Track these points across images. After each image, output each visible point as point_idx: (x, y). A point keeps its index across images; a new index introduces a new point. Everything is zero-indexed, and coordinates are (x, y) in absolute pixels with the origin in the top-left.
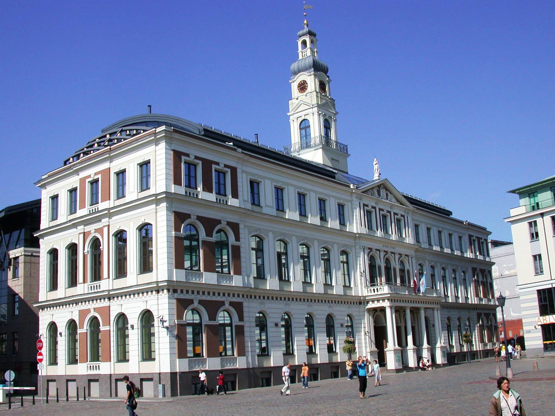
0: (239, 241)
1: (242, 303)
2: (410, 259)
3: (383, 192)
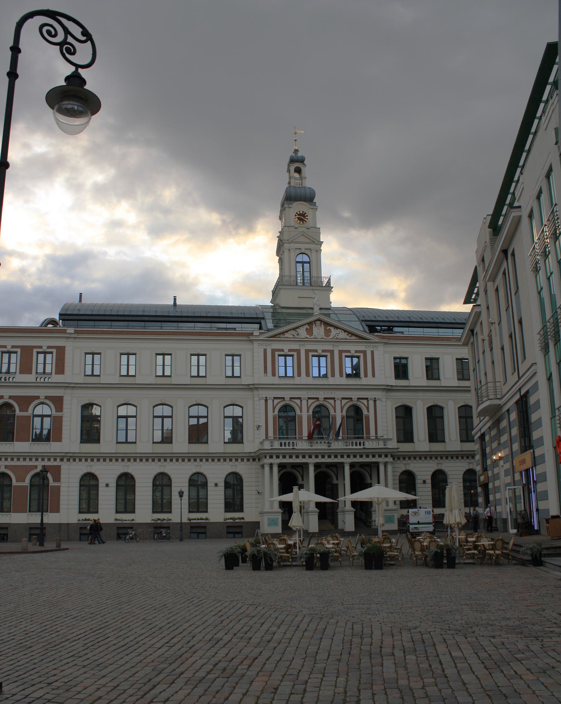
0: (62, 411)
1: (60, 466)
2: (371, 403)
3: (319, 331)
